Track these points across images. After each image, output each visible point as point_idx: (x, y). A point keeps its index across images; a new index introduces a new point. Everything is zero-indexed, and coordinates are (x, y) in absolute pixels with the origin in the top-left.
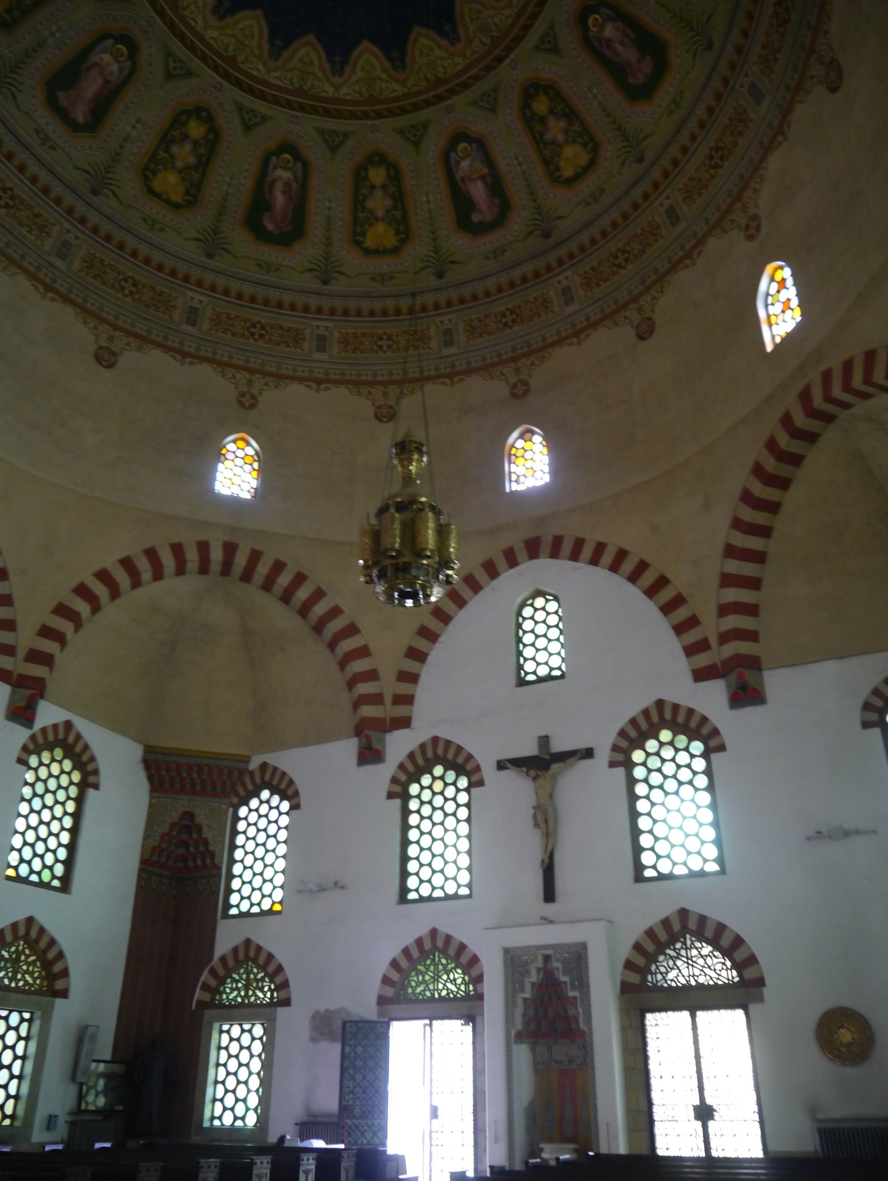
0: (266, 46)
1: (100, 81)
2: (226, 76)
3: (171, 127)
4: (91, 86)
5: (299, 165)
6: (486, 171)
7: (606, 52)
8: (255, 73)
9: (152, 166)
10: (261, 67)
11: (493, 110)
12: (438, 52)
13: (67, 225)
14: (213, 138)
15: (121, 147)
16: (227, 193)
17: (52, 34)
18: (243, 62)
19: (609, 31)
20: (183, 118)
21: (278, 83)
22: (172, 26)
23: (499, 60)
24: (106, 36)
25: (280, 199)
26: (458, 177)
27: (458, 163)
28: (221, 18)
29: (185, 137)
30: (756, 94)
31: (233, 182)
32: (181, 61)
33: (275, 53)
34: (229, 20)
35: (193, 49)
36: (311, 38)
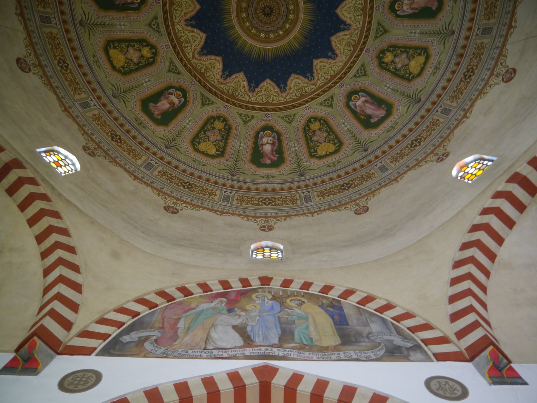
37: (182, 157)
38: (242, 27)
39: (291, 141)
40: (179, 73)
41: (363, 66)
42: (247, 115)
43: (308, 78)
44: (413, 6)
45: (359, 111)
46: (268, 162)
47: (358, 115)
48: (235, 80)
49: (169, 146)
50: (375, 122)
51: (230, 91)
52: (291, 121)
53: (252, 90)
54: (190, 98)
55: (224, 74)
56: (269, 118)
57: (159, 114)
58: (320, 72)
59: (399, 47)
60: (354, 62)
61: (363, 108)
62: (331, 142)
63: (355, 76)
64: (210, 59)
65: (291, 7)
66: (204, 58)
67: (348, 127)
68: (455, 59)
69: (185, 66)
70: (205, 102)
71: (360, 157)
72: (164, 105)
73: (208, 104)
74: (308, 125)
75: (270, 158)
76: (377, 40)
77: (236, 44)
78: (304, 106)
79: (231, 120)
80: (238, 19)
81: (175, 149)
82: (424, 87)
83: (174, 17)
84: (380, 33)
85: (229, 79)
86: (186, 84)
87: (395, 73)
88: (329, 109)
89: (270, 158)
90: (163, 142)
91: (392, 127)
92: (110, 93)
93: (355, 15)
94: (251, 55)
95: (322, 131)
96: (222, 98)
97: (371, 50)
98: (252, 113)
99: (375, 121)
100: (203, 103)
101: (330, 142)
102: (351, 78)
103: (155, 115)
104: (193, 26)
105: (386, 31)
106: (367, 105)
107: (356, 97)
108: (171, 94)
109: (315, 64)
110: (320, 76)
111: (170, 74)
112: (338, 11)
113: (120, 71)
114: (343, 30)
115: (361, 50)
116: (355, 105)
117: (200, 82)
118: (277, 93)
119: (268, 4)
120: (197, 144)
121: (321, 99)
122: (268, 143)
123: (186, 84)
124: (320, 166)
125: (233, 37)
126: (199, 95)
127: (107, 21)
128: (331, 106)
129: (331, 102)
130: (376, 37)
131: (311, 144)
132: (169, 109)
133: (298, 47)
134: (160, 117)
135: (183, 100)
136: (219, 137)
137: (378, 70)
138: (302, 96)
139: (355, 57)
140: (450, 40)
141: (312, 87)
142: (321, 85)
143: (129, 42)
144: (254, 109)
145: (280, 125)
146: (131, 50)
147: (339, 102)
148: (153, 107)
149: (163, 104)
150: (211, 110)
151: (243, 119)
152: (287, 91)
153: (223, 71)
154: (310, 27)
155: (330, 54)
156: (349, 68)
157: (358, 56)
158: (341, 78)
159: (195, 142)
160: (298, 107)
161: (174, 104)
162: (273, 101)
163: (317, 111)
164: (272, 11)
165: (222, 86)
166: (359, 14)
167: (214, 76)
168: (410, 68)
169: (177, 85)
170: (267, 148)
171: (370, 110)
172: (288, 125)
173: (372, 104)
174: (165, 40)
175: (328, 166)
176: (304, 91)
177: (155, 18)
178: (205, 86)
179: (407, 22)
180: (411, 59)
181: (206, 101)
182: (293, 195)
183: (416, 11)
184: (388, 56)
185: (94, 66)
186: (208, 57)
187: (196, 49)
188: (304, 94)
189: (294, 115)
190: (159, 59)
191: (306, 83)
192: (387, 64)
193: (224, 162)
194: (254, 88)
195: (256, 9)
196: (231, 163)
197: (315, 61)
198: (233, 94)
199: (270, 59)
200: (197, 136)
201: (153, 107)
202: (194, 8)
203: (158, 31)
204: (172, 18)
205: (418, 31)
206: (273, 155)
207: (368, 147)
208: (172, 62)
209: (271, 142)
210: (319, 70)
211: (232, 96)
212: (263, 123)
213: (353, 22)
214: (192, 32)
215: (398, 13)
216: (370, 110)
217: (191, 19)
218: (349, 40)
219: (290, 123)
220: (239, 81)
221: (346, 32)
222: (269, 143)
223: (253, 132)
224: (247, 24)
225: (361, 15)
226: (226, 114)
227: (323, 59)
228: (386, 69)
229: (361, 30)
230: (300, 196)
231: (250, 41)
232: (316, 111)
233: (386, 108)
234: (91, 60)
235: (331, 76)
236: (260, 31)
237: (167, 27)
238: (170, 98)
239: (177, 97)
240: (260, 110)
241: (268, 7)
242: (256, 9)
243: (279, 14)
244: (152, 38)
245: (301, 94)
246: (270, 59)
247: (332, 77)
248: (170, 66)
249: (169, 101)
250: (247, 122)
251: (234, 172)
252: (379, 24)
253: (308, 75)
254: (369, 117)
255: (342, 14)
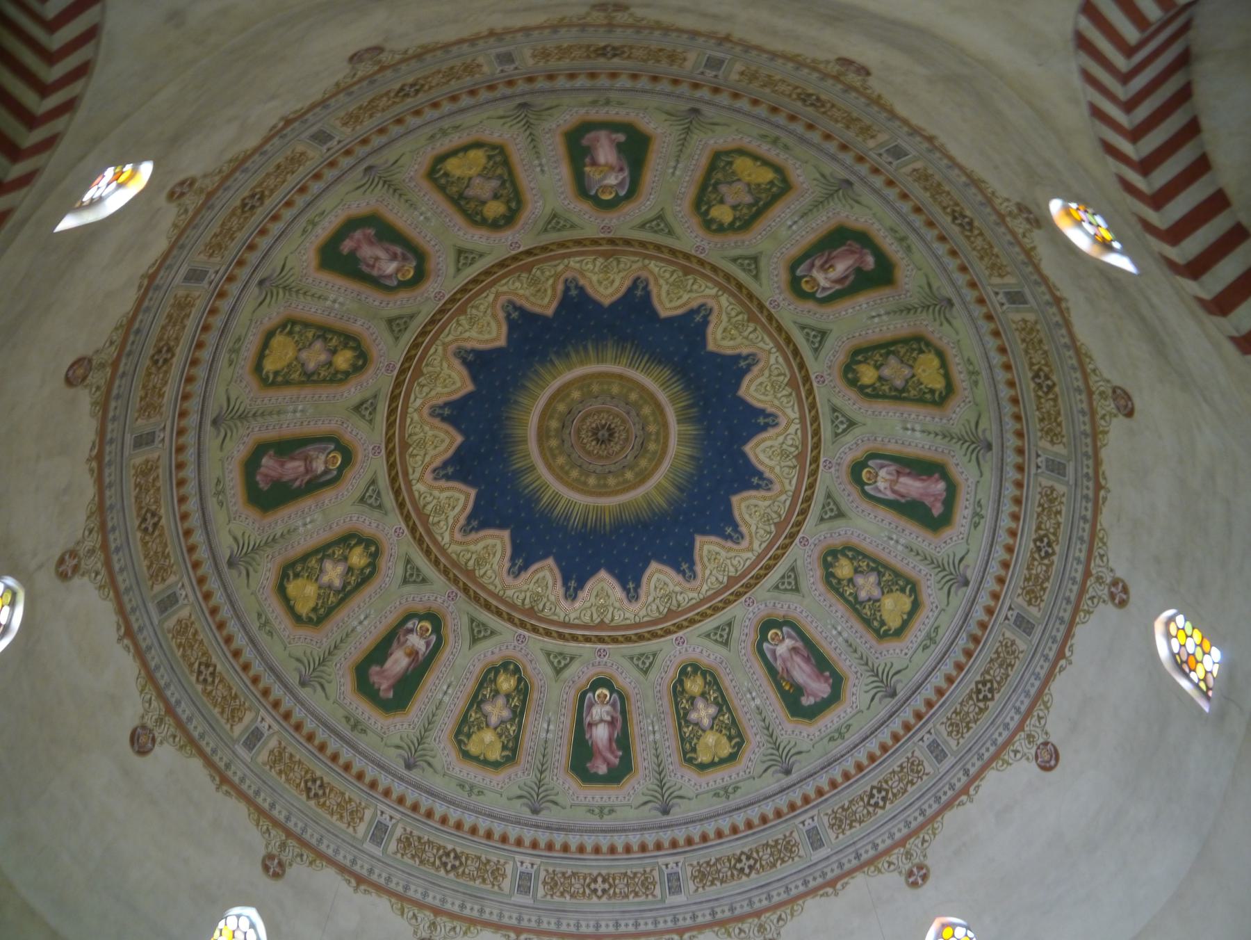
0: (756, 369)
1: (903, 480)
2: (807, 379)
3: (884, 397)
4: (912, 487)
5: (799, 272)
6: (587, 169)
7: (399, 250)
8: (781, 360)
9: (928, 396)
10: (772, 361)
11: (555, 216)
12: (595, 278)
13: (1033, 470)
14: (860, 354)
15: (937, 434)
16: (888, 313)
17: (897, 542)
18: (785, 375)
19: (391, 268)
20: (869, 390)
21: (767, 339)
22: (817, 446)
23: (529, 253)
24: (866, 494)
25: (841, 267)
26: (626, 173)
27: (621, 184)
28: (774, 416)
29: (880, 378)
30: (195, 276)
31: (874, 314)
32: (833, 422)
33: (752, 360)
34: (770, 410)
35: (815, 419)
36: (711, 346)
37: (438, 783)
38: (549, 467)
39: (647, 717)
40: (424, 581)
41: (793, 569)
42: (561, 654)
43: (683, 573)
44: (896, 488)
45: (780, 670)
46: (602, 769)
47: (778, 677)
48: (536, 577)
49: (412, 760)
50: (810, 706)
51: (527, 601)
52: (648, 669)
53: (570, 596)
54: (448, 632)
55: (513, 565)
56: (605, 659)
57: (387, 690)
58: (707, 564)
59: (865, 556)
60: (776, 558)
61: (789, 664)
62: (724, 731)
63: (777, 587)
64: (484, 538)
65: (652, 428)
66: (473, 536)
67: (758, 701)
68: (962, 641)
69: (436, 563)
70: (478, 633)
71: (775, 787)
72: (398, 662)
73: (485, 637)
74: (680, 682)
75: (605, 760)
76: (824, 526)
77: (538, 500)
78: (674, 636)
79: (529, 668)
80: (542, 452)
81: (425, 765)
82: (905, 666)
83: (410, 471)
84: (829, 514)
85: (525, 576)
86: (439, 600)
87: (854, 605)
88: (721, 651)
89: (605, 760)
90: (400, 755)
91: (840, 733)
92: (293, 680)
93: (783, 464)
94: (569, 521)
95: (707, 700)
96: (510, 619)
97: (810, 541)
98: (571, 647)
99: (808, 703)
100: (474, 636)
101: (721, 731)
102: (769, 591)
103: (381, 694)
104: (448, 478)
105: (841, 515)
106: (798, 659)
107: (777, 634)
108: (411, 631)
109: (697, 544)
110: (708, 572)
111: (409, 588)
112: (748, 449)
113: (310, 620)
114: (758, 487)
115: (792, 536)
116: (774, 652)
117: (466, 590)
118: (621, 601)
119: (603, 422)
120: (465, 740)
121: (709, 624)
122: (602, 721)
123: (439, 600)
124: (700, 791)
125: (531, 488)
126: (465, 620)
127: (279, 530)
128: (726, 644)
129: (728, 634)
130: (822, 520)
131: (685, 730)
132: (408, 669)
133: (665, 506)
134: (391, 695)
135: (434, 638)
136: (506, 714)
137: (821, 587)
138: (671, 613)
139: (778, 549)
140: (960, 593)
141: (691, 595)
142: (709, 593)
143: (323, 552)
144: (574, 638)
145: (627, 678)
146: (328, 565)
147: (743, 638)
148: (378, 673)
149: (396, 662)
150: (490, 652)
151: (552, 663)
152: (643, 598)
153: (513, 559)
154: (688, 469)
155: (729, 530)
156: (766, 569)
157: (785, 547)
158: (748, 587)
159: (463, 731)
160: (662, 636)
161: (417, 653)
162: (612, 620)
163: (700, 648)
164: (611, 435)
165: (509, 593)
166: (790, 463)
167: (494, 572)
168: (882, 609)
169: (420, 608)
170: (601, 734)
171: (802, 673)
172: (641, 677)
173: (807, 660)
174: (395, 521)
175: (715, 795)
176: (674, 602)
177: (373, 482)
178: (477, 598)
179: (883, 513)
180: (886, 591)
181: (479, 632)
182: (648, 870)
183: (903, 501)
184: (842, 566)
185: (262, 638)
186: (482, 533)
187: (456, 520)
188: (674, 608)
189: (654, 655)
190: (383, 563)
191: (679, 584)
192: (839, 581)
193: (519, 777)
194: (576, 590)
195: (578, 431)
196: (531, 778)
197: (699, 539)
198: (532, 608)
199: (608, 528)
200: (464, 720)
201: (378, 673)
202: (452, 443)
203: (380, 507)
204: (406, 474)
205: (902, 541)
206: (612, 752)
207: (793, 764)
208: (408, 561)
209: (609, 718)
210: (705, 560)
211: (531, 612)
212: (591, 673)
213: (777, 476)
214: (448, 489)
215: (866, 488)
216: (802, 673)
217: (445, 464)
218: (768, 510)
219: (645, 672)
220: (544, 578)
221: (763, 493)
222: (605, 721)
223: (572, 696)
224: (561, 460)
225: (795, 467)
226: (519, 655)
227: (713, 539)
228: (836, 590)
229: (793, 496)
230: (661, 871)
231: (568, 494)
232: (698, 650)
233: (831, 681)
234: (254, 627)
235: (729, 578)
236: (588, 474)
237: (397, 493)
238: (409, 643)
239: (421, 636)
240: (587, 639)
241: (603, 427)
242: (578, 431)
243: (627, 440)
244: (367, 523)
245: (669, 609)
246: (608, 528)
247: (732, 580)
248: (406, 571)
249: (408, 651)
250: (562, 669)
251: (537, 800)
252: (829, 496)
253: (685, 566)
254: (799, 690)
255: (757, 457)
